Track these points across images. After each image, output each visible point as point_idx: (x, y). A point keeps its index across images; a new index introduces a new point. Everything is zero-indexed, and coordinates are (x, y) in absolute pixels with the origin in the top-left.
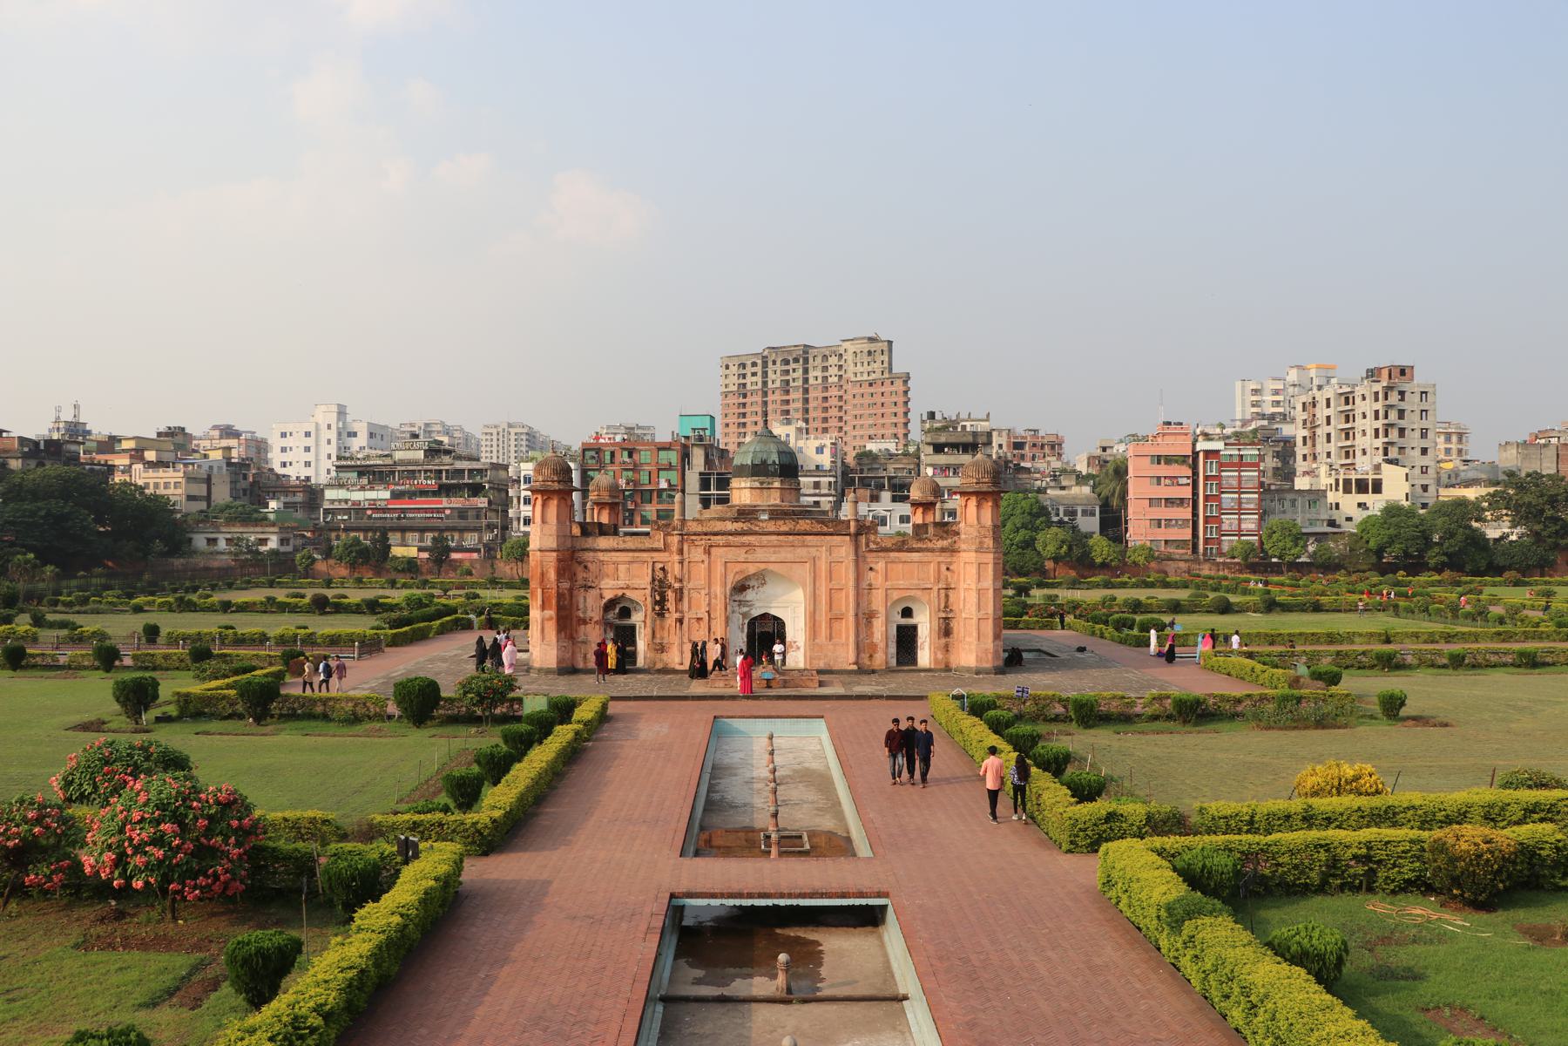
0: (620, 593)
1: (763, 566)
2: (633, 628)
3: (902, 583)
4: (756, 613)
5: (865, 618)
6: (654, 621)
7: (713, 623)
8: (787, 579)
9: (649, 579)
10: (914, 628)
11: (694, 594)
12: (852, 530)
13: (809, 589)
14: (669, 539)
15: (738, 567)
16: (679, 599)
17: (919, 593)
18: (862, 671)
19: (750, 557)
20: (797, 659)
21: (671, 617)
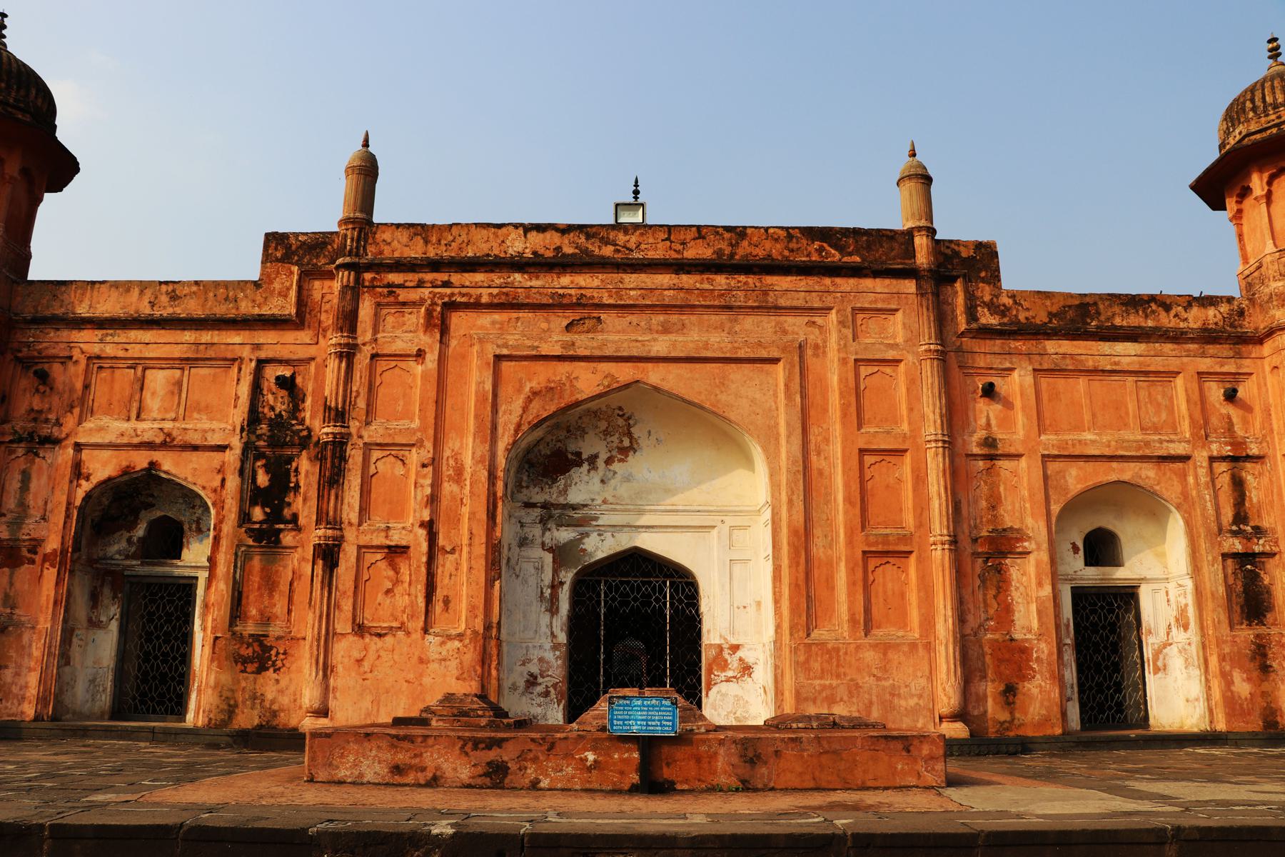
0: (140, 460)
1: (625, 373)
2: (186, 589)
3: (1092, 440)
4: (600, 547)
5: (983, 554)
6: (241, 559)
7: (446, 564)
8: (712, 429)
9: (239, 415)
10: (1128, 596)
11: (384, 466)
12: (922, 258)
13: (788, 449)
14: (318, 288)
15: (541, 375)
16: (332, 479)
17: (1148, 473)
18: (987, 745)
19: (584, 343)
20: (741, 699)
21: (299, 558)
